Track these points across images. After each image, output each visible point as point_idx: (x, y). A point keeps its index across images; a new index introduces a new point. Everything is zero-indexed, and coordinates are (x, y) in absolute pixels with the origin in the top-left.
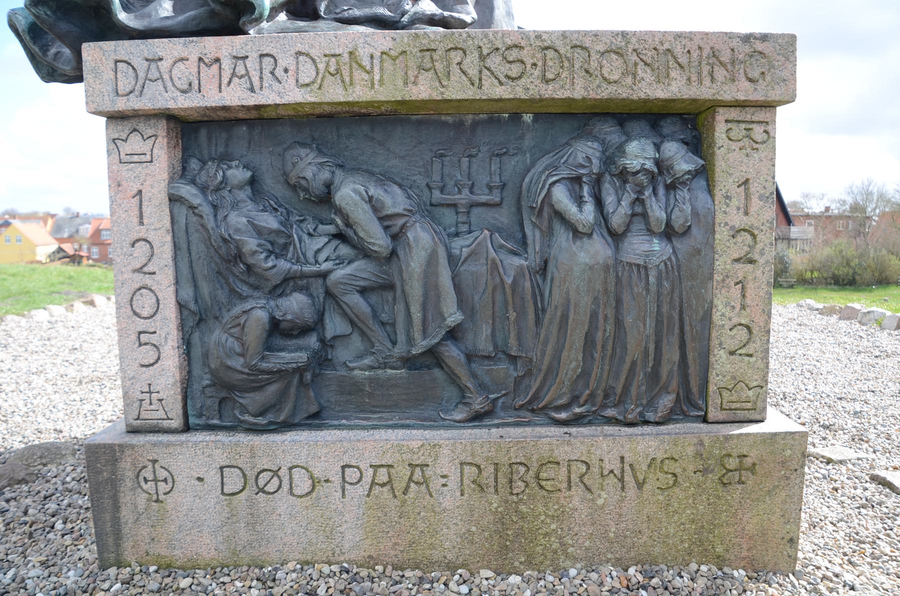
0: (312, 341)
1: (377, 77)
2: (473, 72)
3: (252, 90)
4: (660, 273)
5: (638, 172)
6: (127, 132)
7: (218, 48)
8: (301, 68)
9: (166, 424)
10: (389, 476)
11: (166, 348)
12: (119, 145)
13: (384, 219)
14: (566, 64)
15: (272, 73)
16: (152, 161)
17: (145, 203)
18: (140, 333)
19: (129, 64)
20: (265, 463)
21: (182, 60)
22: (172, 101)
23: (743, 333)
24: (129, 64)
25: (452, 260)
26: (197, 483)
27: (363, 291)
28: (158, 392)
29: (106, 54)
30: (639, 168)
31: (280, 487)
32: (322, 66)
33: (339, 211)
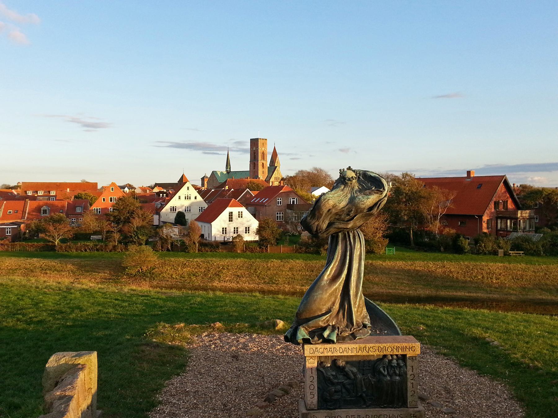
0: (340, 393)
25: (364, 380)
33: (345, 371)
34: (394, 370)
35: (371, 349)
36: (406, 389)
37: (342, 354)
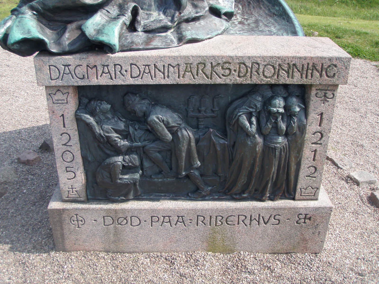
1: (166, 74)
2: (208, 73)
3: (111, 78)
4: (281, 150)
5: (275, 113)
6: (55, 91)
7: (95, 62)
8: (133, 70)
9: (79, 199)
10: (169, 220)
11: (78, 173)
12: (52, 96)
13: (170, 128)
14: (249, 70)
15: (120, 72)
16: (67, 103)
17: (65, 120)
18: (66, 168)
19: (56, 67)
20: (121, 215)
21: (79, 65)
22: (76, 83)
23: (313, 169)
24: (56, 67)
26: (94, 221)
27: (159, 152)
28: (75, 188)
29: (45, 63)
30: (276, 111)
31: (127, 223)
32: (142, 70)
34: (276, 123)
35: (219, 69)
36: (299, 165)
37: (138, 82)
